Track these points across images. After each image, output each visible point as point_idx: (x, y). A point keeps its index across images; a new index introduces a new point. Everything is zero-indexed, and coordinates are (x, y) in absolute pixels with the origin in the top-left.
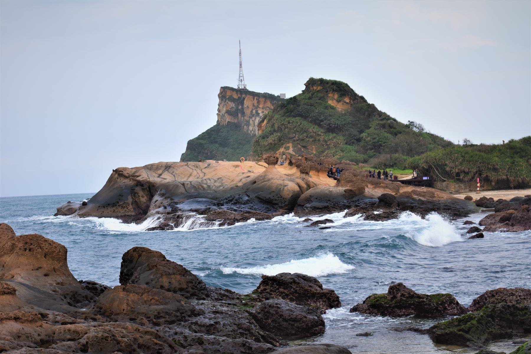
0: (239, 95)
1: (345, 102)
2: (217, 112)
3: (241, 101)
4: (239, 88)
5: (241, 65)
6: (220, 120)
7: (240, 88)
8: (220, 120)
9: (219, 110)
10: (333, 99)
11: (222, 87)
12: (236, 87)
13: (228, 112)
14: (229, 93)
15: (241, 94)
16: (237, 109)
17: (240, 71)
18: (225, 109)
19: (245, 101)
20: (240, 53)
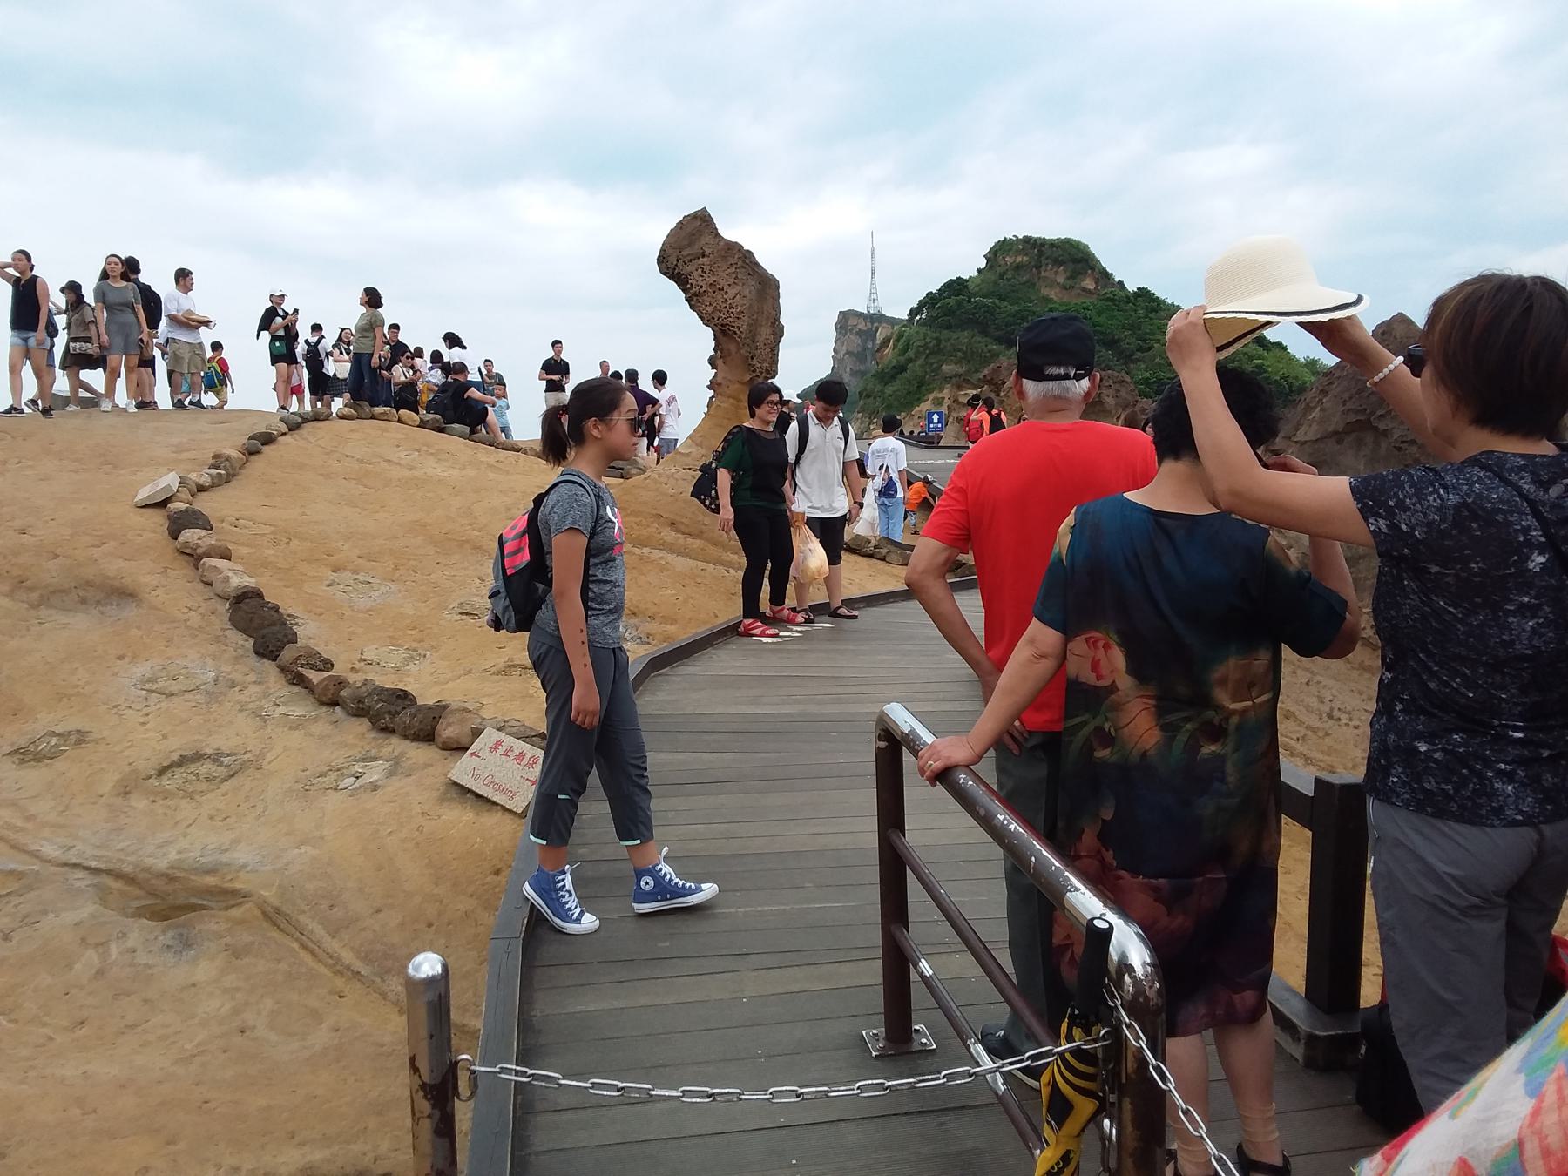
0: (869, 325)
1: (1084, 289)
2: (833, 354)
3: (871, 334)
4: (869, 312)
5: (873, 273)
6: (836, 366)
7: (872, 312)
8: (836, 366)
9: (835, 350)
10: (1052, 284)
11: (840, 312)
12: (866, 312)
13: (848, 353)
14: (853, 321)
15: (872, 324)
16: (865, 349)
17: (872, 284)
18: (844, 348)
19: (878, 334)
20: (873, 253)
